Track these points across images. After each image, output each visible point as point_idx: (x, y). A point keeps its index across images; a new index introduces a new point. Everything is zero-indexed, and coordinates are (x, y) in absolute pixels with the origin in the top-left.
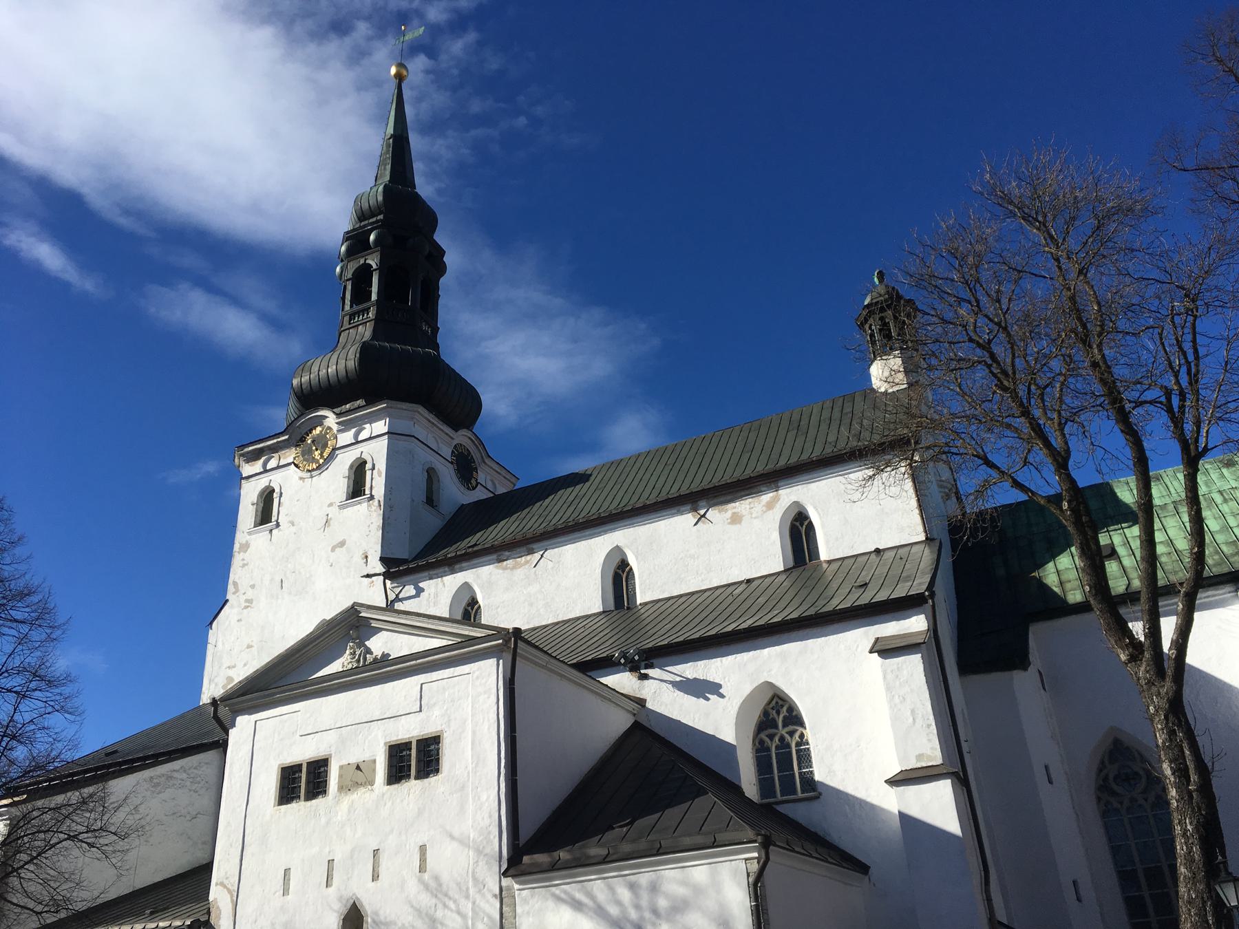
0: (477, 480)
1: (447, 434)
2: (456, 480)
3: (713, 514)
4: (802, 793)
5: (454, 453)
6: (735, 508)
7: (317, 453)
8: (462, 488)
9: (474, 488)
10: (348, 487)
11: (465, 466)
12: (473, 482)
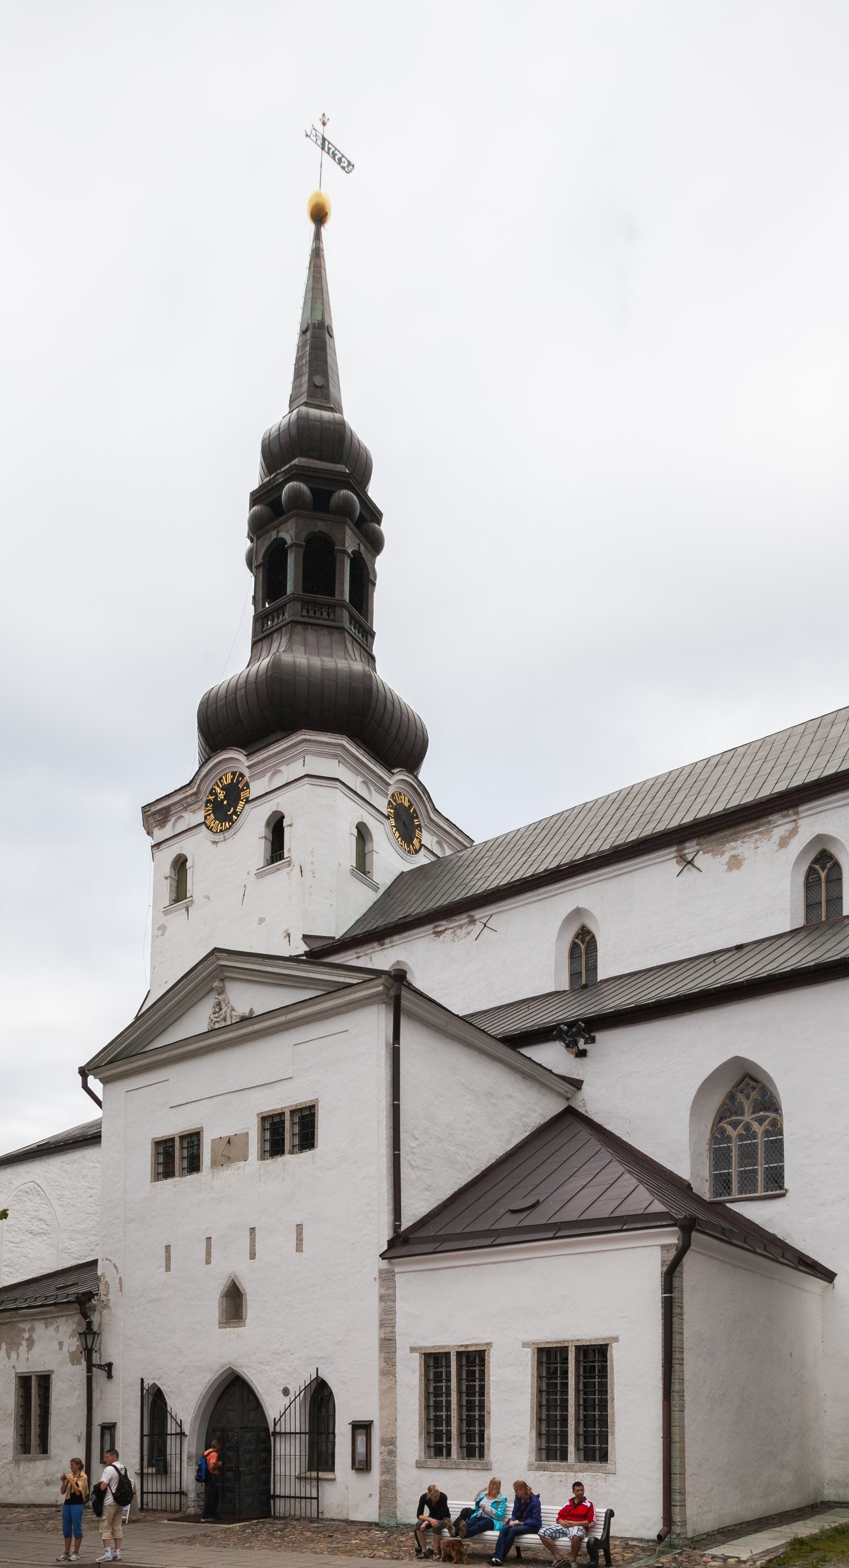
3: (702, 860)
6: (735, 848)
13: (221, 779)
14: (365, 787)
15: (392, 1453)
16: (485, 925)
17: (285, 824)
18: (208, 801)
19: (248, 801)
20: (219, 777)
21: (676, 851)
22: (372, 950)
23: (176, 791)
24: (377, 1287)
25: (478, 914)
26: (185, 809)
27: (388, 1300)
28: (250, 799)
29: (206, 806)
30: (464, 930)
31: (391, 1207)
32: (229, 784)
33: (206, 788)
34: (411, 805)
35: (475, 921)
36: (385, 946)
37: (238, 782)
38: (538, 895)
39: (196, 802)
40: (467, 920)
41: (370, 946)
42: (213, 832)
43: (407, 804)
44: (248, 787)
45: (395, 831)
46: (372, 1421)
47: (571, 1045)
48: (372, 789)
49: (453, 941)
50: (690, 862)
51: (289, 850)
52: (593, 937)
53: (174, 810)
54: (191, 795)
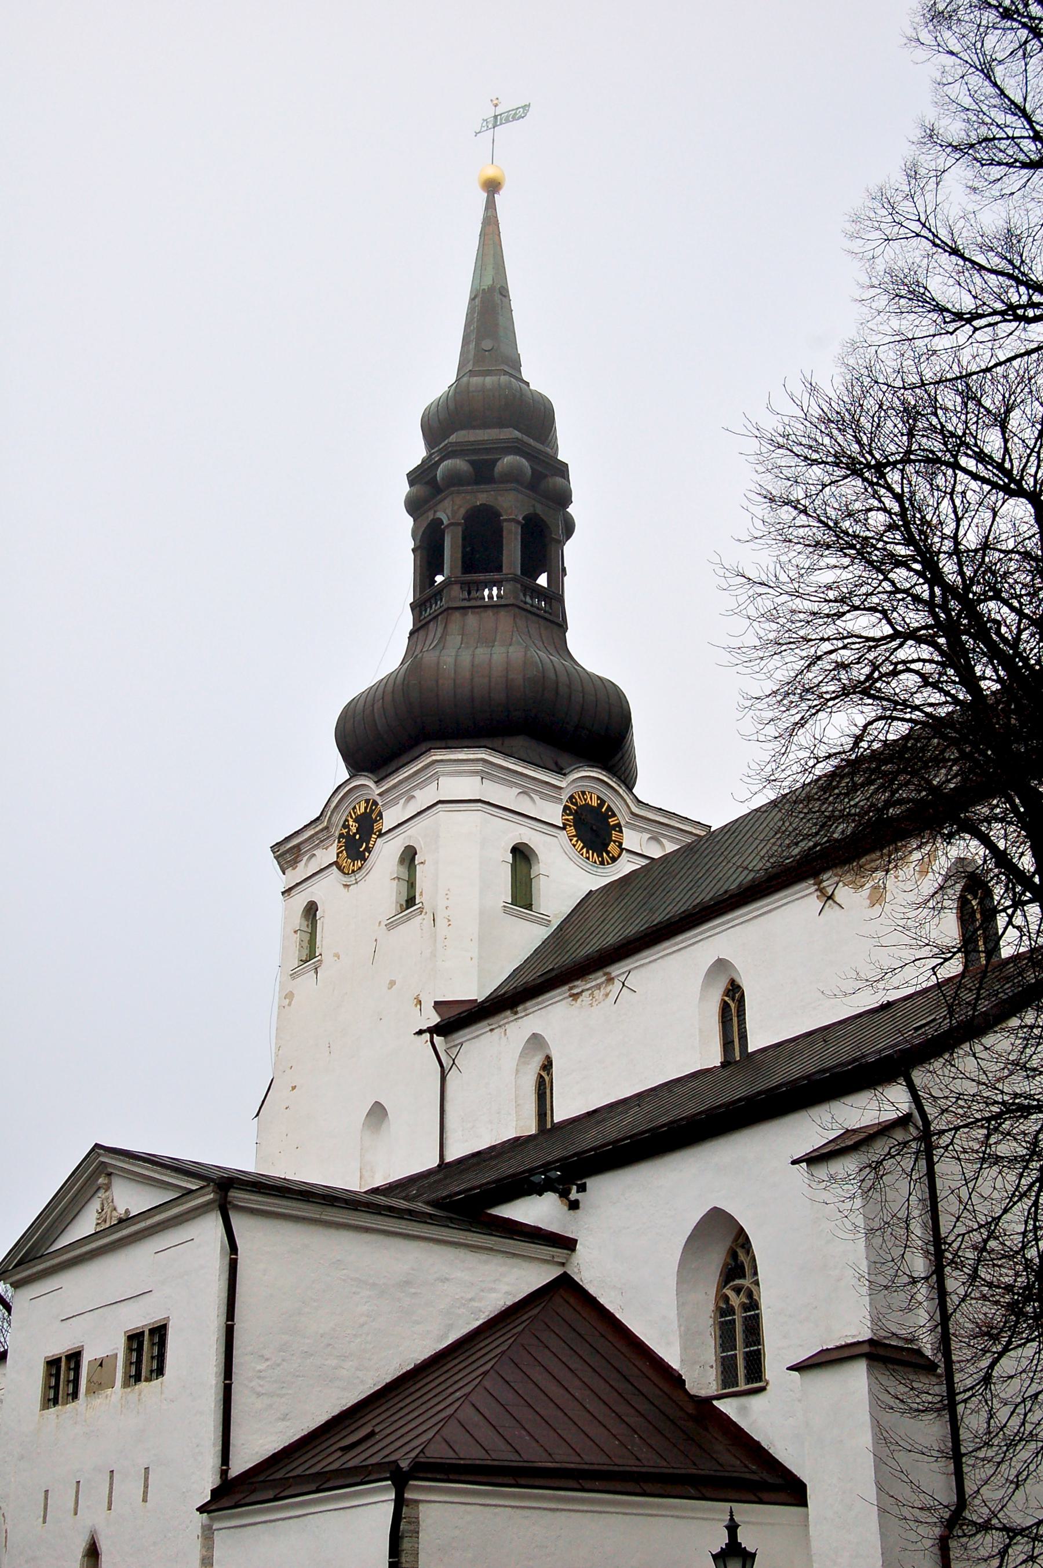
0: (621, 844)
2: (573, 853)
3: (843, 893)
4: (748, 1383)
9: (614, 859)
12: (612, 847)
13: (355, 808)
14: (526, 797)
16: (623, 984)
17: (416, 862)
18: (341, 836)
19: (381, 835)
20: (352, 806)
21: (814, 884)
22: (505, 1021)
23: (305, 826)
24: (199, 1547)
25: (617, 970)
28: (383, 831)
29: (339, 842)
30: (603, 991)
31: (219, 1448)
32: (363, 813)
33: (339, 819)
34: (603, 802)
35: (613, 979)
36: (519, 1015)
37: (372, 811)
39: (328, 838)
40: (604, 978)
41: (503, 1015)
42: (345, 873)
43: (595, 803)
44: (381, 818)
45: (577, 841)
47: (564, 1194)
49: (591, 1005)
50: (830, 898)
51: (421, 894)
52: (743, 995)
54: (322, 830)
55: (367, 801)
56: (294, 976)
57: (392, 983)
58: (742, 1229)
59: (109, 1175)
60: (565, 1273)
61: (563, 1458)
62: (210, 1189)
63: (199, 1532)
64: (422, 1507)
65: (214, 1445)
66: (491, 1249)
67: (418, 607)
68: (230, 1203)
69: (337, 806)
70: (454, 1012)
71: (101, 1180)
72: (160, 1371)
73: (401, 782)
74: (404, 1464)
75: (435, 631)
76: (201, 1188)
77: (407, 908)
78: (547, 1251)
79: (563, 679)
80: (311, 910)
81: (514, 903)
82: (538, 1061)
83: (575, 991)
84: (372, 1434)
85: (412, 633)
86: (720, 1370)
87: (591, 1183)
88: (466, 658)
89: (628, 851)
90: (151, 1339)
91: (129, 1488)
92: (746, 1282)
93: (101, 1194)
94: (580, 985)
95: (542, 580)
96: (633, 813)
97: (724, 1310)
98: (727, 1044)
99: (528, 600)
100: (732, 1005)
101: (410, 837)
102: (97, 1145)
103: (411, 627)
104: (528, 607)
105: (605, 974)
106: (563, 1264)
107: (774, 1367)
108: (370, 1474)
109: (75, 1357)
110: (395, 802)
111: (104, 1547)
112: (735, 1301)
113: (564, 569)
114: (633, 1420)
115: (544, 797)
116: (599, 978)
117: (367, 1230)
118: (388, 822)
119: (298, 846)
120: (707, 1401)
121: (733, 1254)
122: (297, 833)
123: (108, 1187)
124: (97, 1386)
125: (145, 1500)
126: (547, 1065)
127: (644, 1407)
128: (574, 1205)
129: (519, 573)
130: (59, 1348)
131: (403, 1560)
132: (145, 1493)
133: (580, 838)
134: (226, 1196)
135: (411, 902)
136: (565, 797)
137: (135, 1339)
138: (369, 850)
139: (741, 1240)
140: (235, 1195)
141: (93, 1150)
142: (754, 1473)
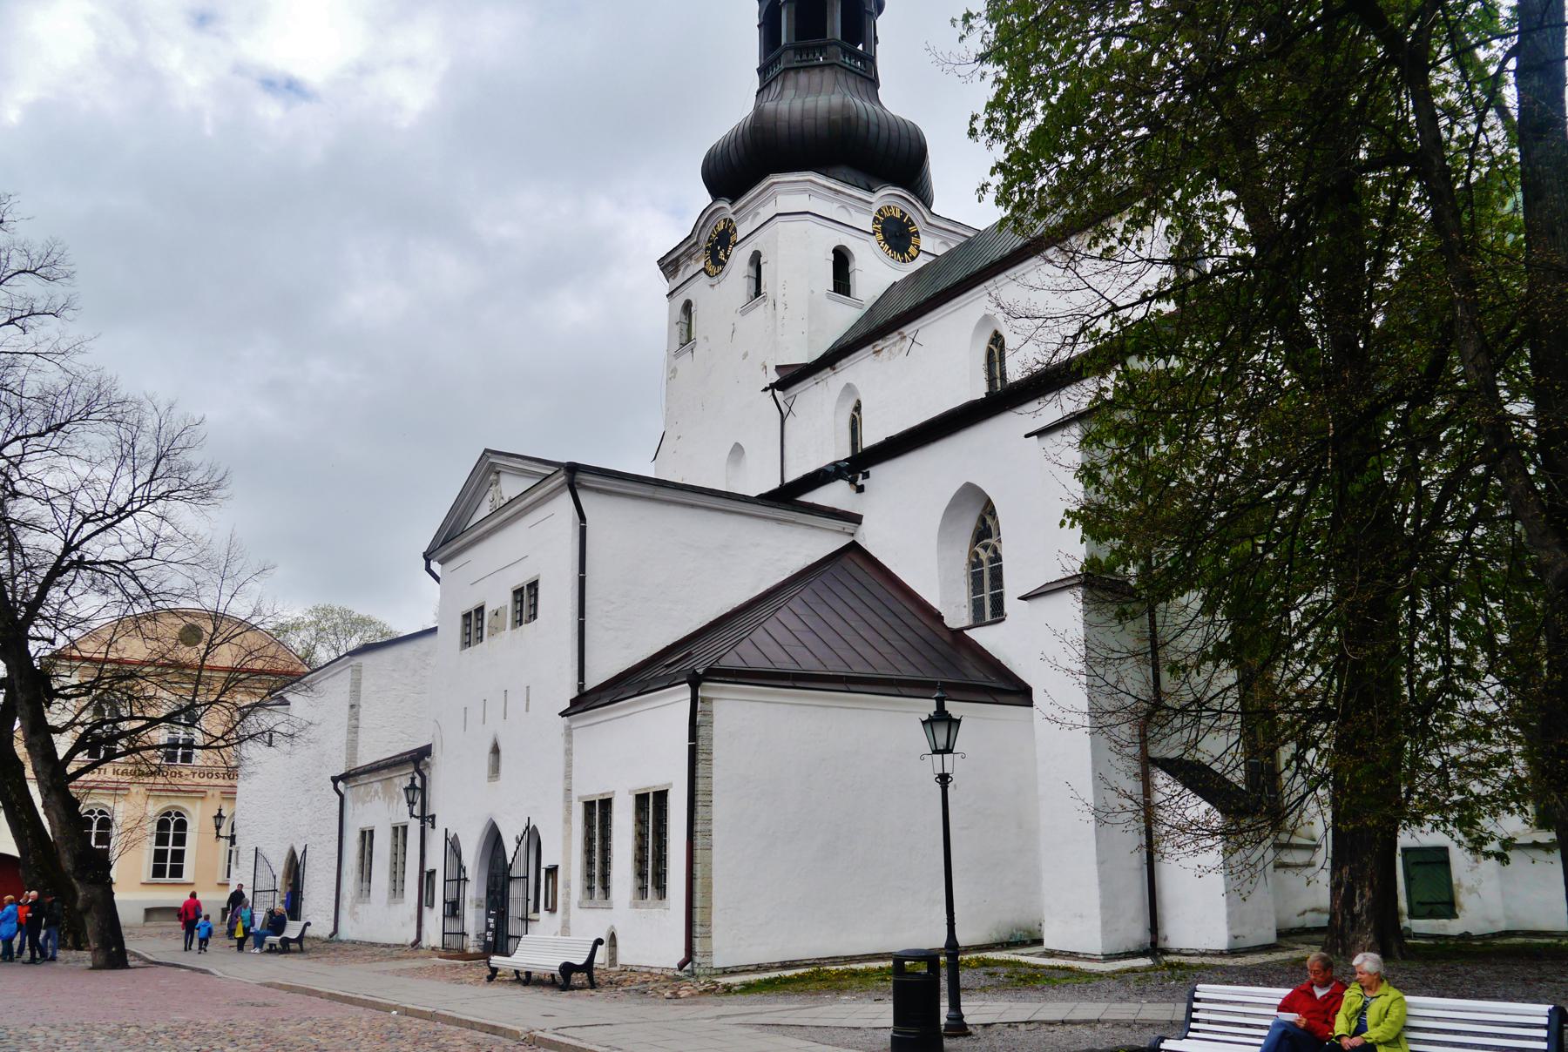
0: (918, 247)
1: (860, 199)
2: (882, 254)
5: (878, 219)
7: (722, 254)
8: (893, 263)
9: (913, 258)
10: (749, 287)
11: (897, 235)
12: (912, 249)
15: (568, 894)
18: (707, 248)
19: (736, 244)
25: (908, 330)
26: (690, 258)
27: (568, 752)
30: (898, 348)
33: (704, 237)
35: (905, 337)
37: (729, 227)
38: (954, 306)
41: (823, 372)
46: (556, 867)
47: (853, 482)
48: (852, 211)
49: (890, 359)
51: (765, 287)
53: (683, 259)
55: (725, 220)
56: (677, 355)
57: (745, 355)
58: (989, 501)
59: (498, 473)
60: (854, 541)
61: (835, 667)
62: (562, 472)
63: (563, 731)
64: (715, 703)
65: (572, 666)
66: (794, 522)
67: (762, 71)
68: (578, 483)
69: (703, 226)
70: (791, 371)
71: (493, 477)
72: (535, 616)
73: (749, 202)
74: (700, 671)
75: (775, 88)
76: (556, 472)
77: (756, 297)
78: (839, 524)
79: (873, 118)
80: (687, 307)
81: (835, 291)
82: (852, 404)
83: (878, 348)
84: (690, 654)
85: (758, 92)
86: (972, 608)
87: (873, 471)
88: (797, 104)
89: (924, 252)
90: (529, 592)
91: (517, 702)
92: (992, 541)
93: (492, 488)
94: (880, 344)
95: (860, 47)
96: (927, 223)
97: (975, 563)
98: (991, 380)
99: (847, 60)
100: (996, 350)
101: (756, 244)
102: (486, 450)
103: (758, 87)
104: (847, 66)
105: (900, 334)
106: (852, 535)
107: (1011, 603)
108: (675, 679)
109: (480, 610)
110: (745, 218)
111: (502, 747)
112: (984, 556)
113: (876, 38)
114: (898, 643)
115: (859, 210)
116: (894, 337)
117: (693, 506)
118: (740, 234)
119: (677, 259)
120: (961, 630)
121: (983, 520)
122: (675, 249)
123: (497, 482)
124: (495, 630)
125: (527, 710)
126: (858, 408)
127: (908, 635)
128: (860, 489)
129: (839, 37)
130: (470, 606)
131: (700, 743)
132: (527, 705)
133: (886, 240)
134: (573, 478)
135: (758, 293)
136: (875, 210)
137: (518, 592)
138: (727, 257)
139: (989, 509)
140: (582, 477)
141: (484, 454)
142: (995, 682)
